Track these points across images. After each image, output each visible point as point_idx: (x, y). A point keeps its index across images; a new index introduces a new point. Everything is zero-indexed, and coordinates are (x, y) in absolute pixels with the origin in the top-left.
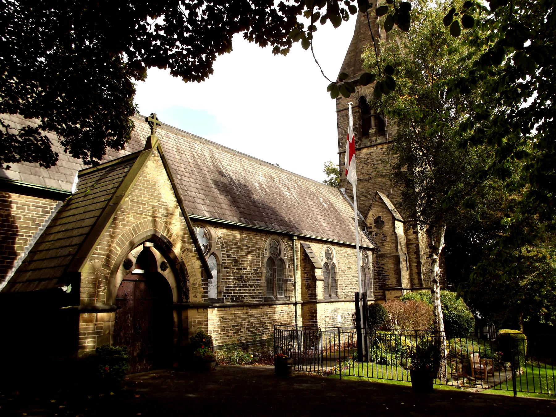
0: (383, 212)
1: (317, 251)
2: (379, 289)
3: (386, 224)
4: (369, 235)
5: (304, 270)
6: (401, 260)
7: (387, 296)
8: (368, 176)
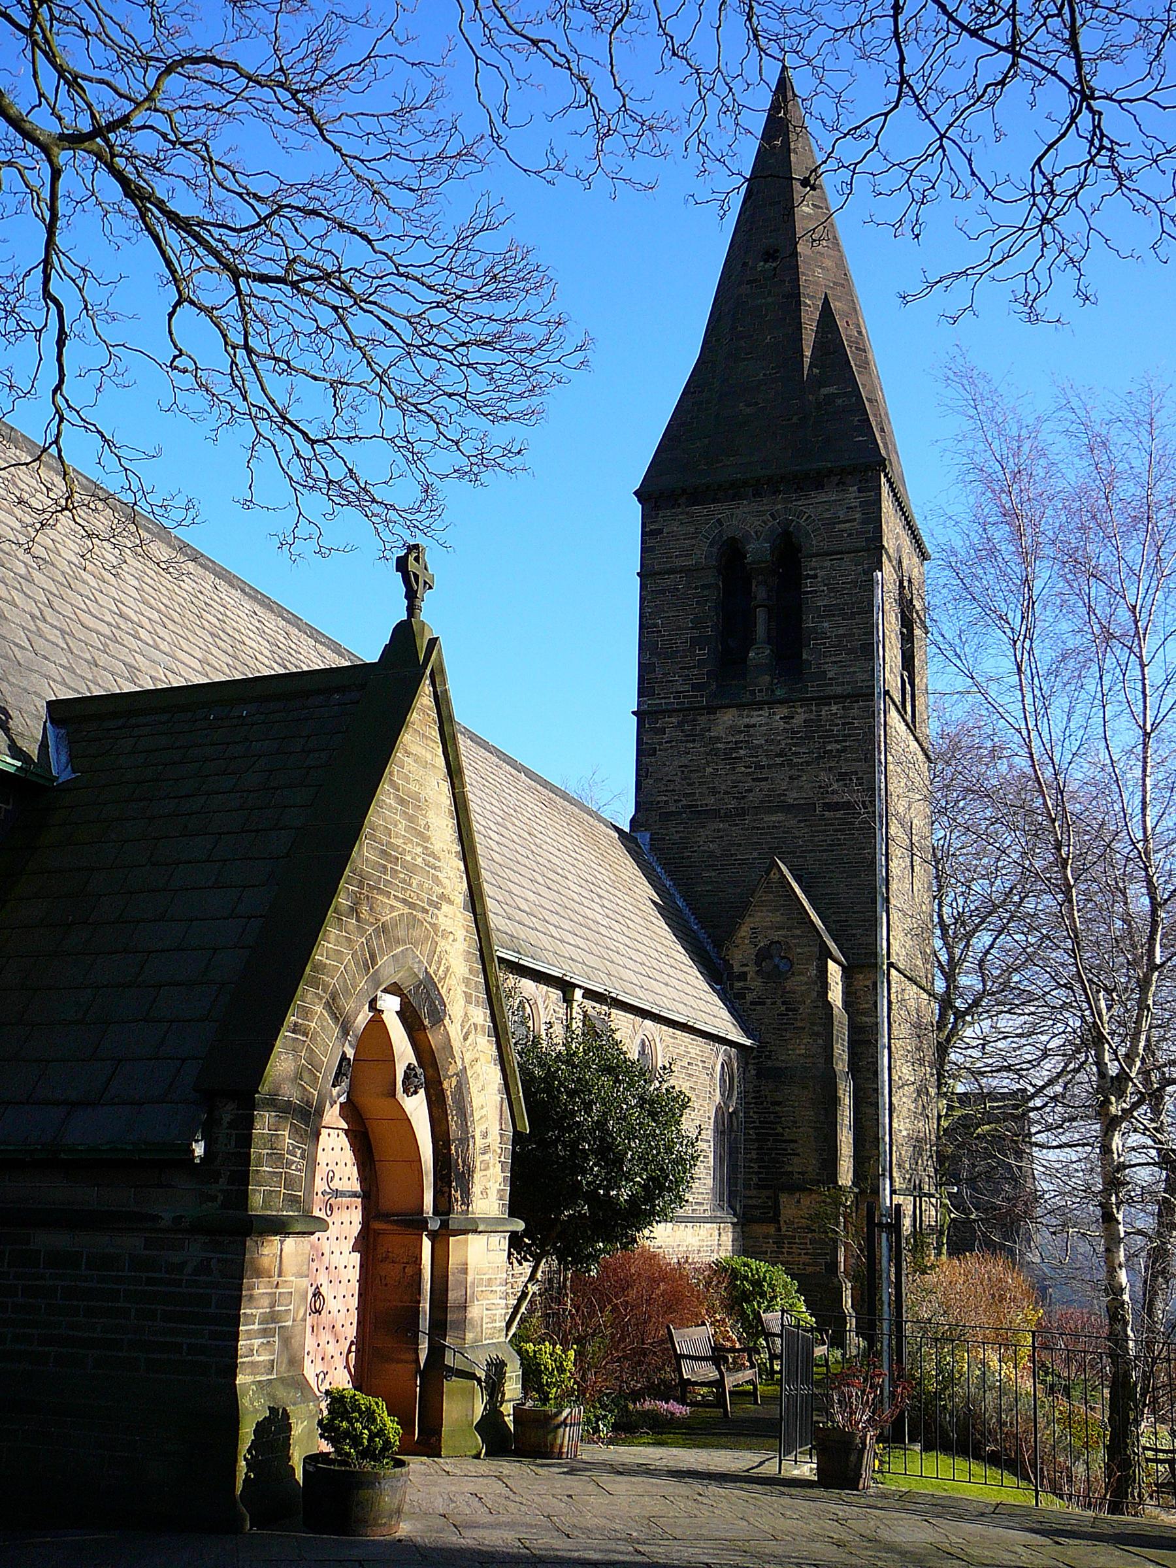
0: (789, 929)
2: (758, 1187)
8: (733, 803)
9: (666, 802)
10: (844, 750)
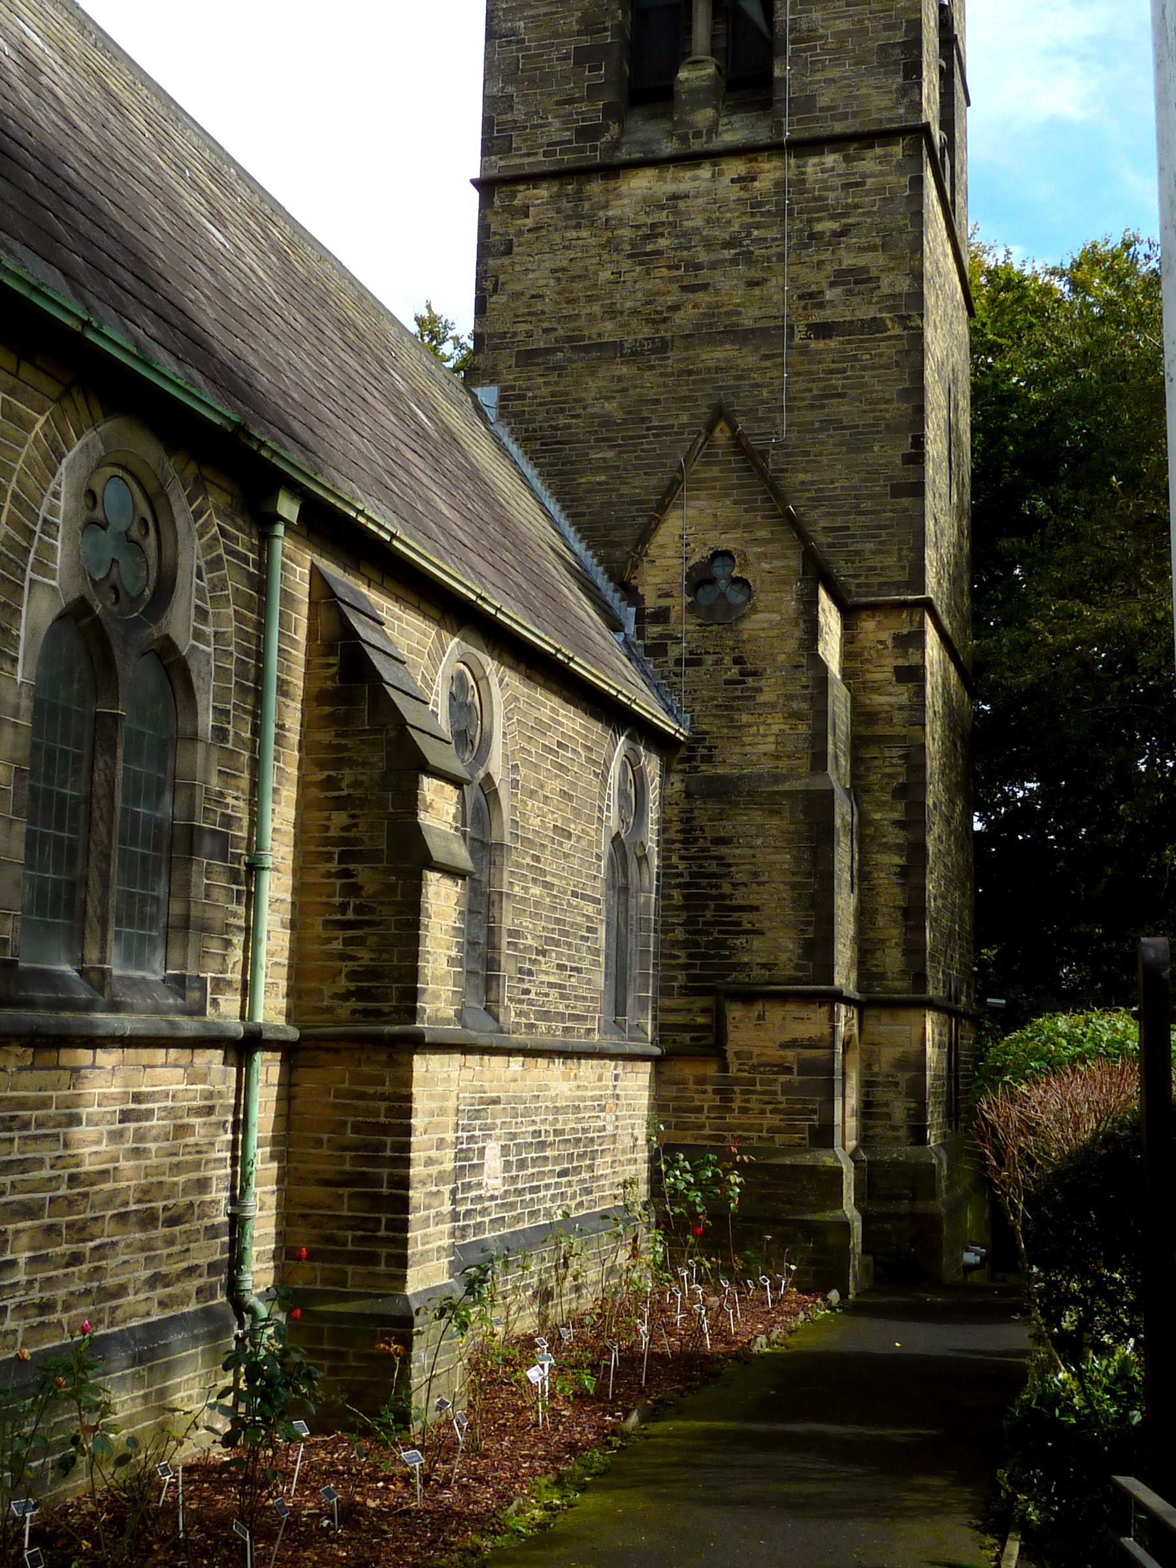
0: (748, 527)
1: (419, 654)
2: (687, 991)
3: (762, 598)
4: (649, 652)
5: (330, 783)
6: (838, 822)
7: (731, 1036)
8: (646, 331)
9: (529, 334)
10: (844, 232)
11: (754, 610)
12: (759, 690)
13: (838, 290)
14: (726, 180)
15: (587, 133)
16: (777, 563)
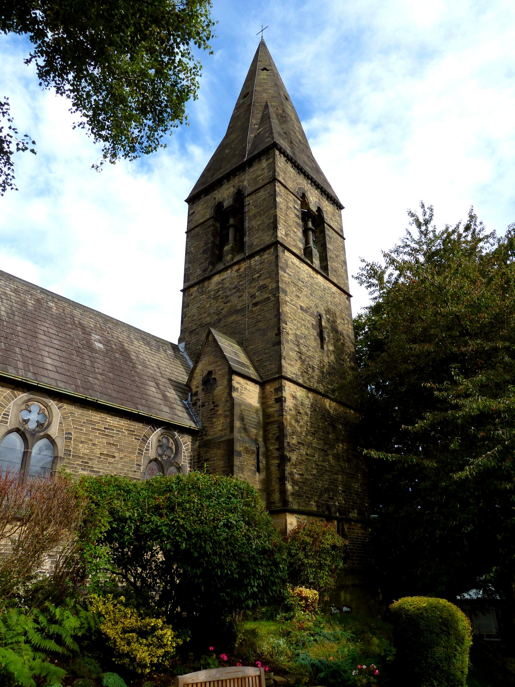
11: (217, 387)
12: (218, 410)
13: (259, 292)
14: (234, 272)
15: (204, 271)
16: (222, 371)
